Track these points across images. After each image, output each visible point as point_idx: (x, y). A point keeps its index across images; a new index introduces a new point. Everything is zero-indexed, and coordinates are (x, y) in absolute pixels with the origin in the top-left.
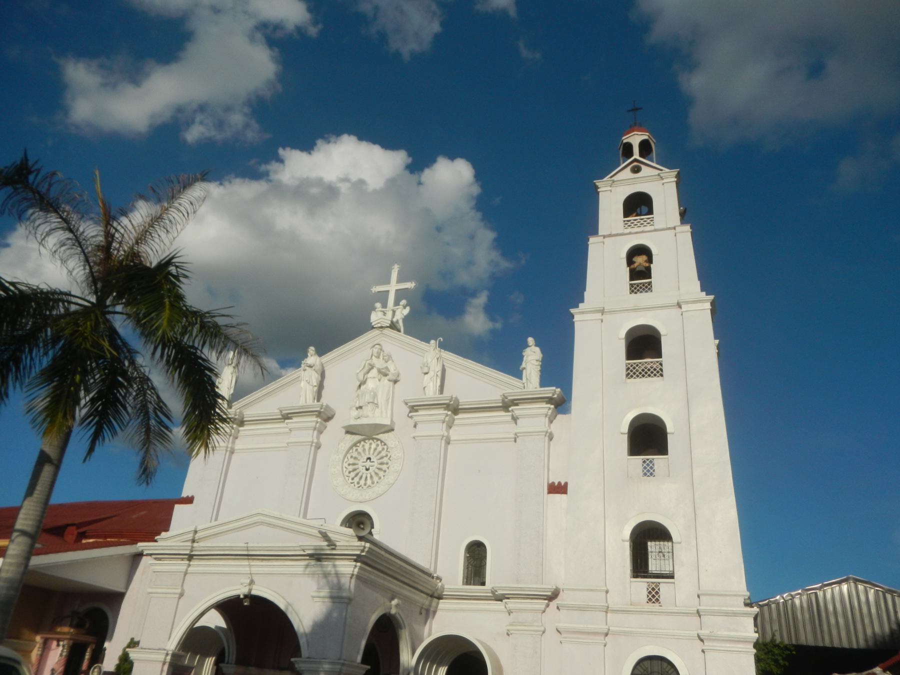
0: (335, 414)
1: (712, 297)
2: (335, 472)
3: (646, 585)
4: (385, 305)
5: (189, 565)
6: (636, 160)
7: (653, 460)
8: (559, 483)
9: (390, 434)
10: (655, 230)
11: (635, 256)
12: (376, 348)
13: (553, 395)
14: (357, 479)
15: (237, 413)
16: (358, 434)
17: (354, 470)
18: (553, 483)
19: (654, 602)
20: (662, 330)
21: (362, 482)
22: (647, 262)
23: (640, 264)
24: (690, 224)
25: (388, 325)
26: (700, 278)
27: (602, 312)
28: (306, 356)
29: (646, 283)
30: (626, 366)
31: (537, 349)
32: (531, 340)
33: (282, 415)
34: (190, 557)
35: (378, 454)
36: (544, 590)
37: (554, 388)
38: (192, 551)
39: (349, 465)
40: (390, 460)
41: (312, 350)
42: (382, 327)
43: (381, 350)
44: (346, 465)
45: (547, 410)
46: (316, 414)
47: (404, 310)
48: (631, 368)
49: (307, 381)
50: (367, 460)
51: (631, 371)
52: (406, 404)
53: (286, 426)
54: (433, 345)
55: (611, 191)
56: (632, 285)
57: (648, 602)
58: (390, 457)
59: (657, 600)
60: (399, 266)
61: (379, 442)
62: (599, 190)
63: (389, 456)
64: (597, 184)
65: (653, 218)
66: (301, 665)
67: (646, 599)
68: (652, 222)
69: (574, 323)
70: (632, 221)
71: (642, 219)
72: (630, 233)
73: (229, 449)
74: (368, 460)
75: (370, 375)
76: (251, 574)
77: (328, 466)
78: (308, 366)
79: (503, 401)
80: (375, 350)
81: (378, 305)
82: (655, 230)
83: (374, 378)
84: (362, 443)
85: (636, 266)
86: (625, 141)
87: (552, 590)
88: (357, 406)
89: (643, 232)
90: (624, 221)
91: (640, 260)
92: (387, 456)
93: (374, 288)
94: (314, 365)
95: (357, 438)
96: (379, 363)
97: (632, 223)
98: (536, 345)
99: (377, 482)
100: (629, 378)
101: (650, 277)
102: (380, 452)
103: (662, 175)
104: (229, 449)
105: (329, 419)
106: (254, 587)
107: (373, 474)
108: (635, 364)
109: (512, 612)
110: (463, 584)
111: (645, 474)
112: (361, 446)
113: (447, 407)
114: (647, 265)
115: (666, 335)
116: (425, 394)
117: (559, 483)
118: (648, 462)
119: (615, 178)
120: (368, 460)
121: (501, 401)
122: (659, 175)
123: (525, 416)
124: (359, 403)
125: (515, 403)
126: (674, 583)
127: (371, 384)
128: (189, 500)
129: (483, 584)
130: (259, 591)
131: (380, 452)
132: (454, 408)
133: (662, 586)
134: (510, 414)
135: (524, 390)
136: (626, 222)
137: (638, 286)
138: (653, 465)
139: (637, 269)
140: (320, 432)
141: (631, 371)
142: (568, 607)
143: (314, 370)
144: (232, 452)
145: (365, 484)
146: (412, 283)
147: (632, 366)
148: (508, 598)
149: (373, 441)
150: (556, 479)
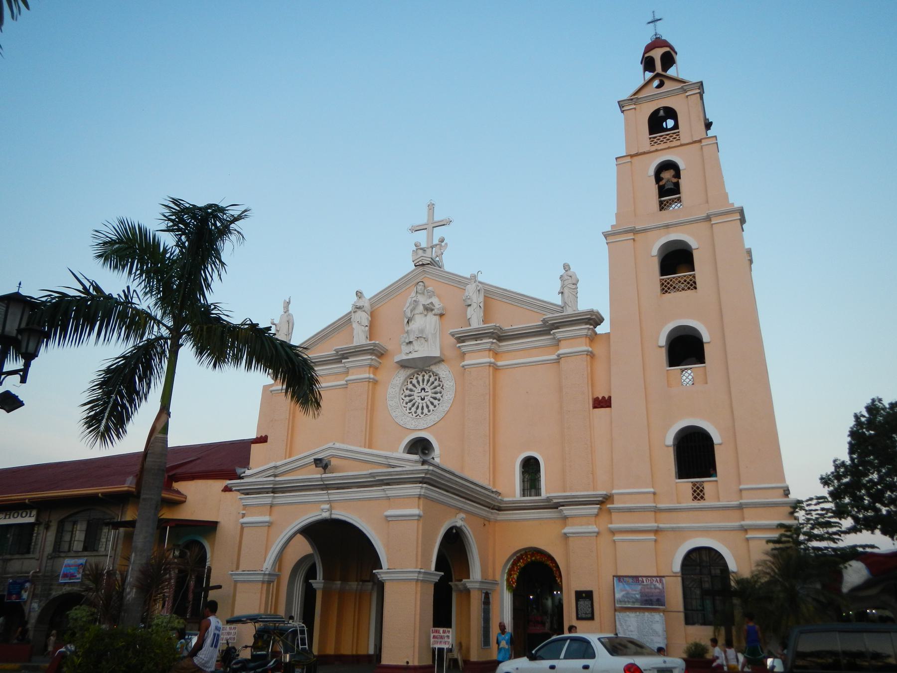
3: (690, 485)
6: (658, 75)
8: (604, 398)
10: (682, 145)
11: (662, 171)
12: (420, 285)
14: (414, 409)
17: (411, 401)
18: (598, 398)
19: (699, 500)
20: (693, 243)
21: (419, 411)
22: (675, 178)
23: (668, 180)
25: (429, 262)
29: (675, 199)
30: (661, 281)
34: (274, 491)
35: (431, 385)
39: (405, 396)
40: (443, 389)
42: (423, 265)
44: (403, 397)
48: (665, 284)
50: (421, 392)
51: (666, 286)
52: (453, 336)
53: (343, 365)
55: (635, 109)
56: (661, 203)
57: (693, 500)
58: (443, 386)
59: (702, 497)
63: (441, 386)
65: (679, 132)
66: (382, 576)
67: (692, 497)
68: (678, 137)
70: (658, 138)
72: (657, 150)
74: (423, 391)
75: (416, 311)
77: (386, 399)
82: (682, 145)
87: (603, 496)
88: (407, 341)
89: (669, 148)
90: (650, 138)
91: (667, 175)
92: (439, 385)
95: (409, 372)
96: (423, 300)
99: (433, 410)
100: (664, 293)
101: (679, 193)
102: (433, 383)
106: (333, 512)
107: (429, 403)
108: (668, 279)
110: (520, 496)
112: (414, 378)
113: (491, 335)
114: (675, 180)
116: (470, 325)
117: (604, 398)
119: (640, 95)
120: (423, 391)
122: (682, 88)
123: (566, 339)
125: (556, 326)
126: (716, 481)
129: (538, 493)
130: (340, 514)
131: (433, 383)
132: (501, 336)
133: (706, 485)
135: (563, 314)
136: (652, 139)
137: (667, 202)
139: (667, 187)
141: (666, 286)
142: (619, 509)
143: (364, 311)
145: (422, 413)
147: (666, 281)
148: (563, 506)
149: (426, 372)
150: (601, 394)
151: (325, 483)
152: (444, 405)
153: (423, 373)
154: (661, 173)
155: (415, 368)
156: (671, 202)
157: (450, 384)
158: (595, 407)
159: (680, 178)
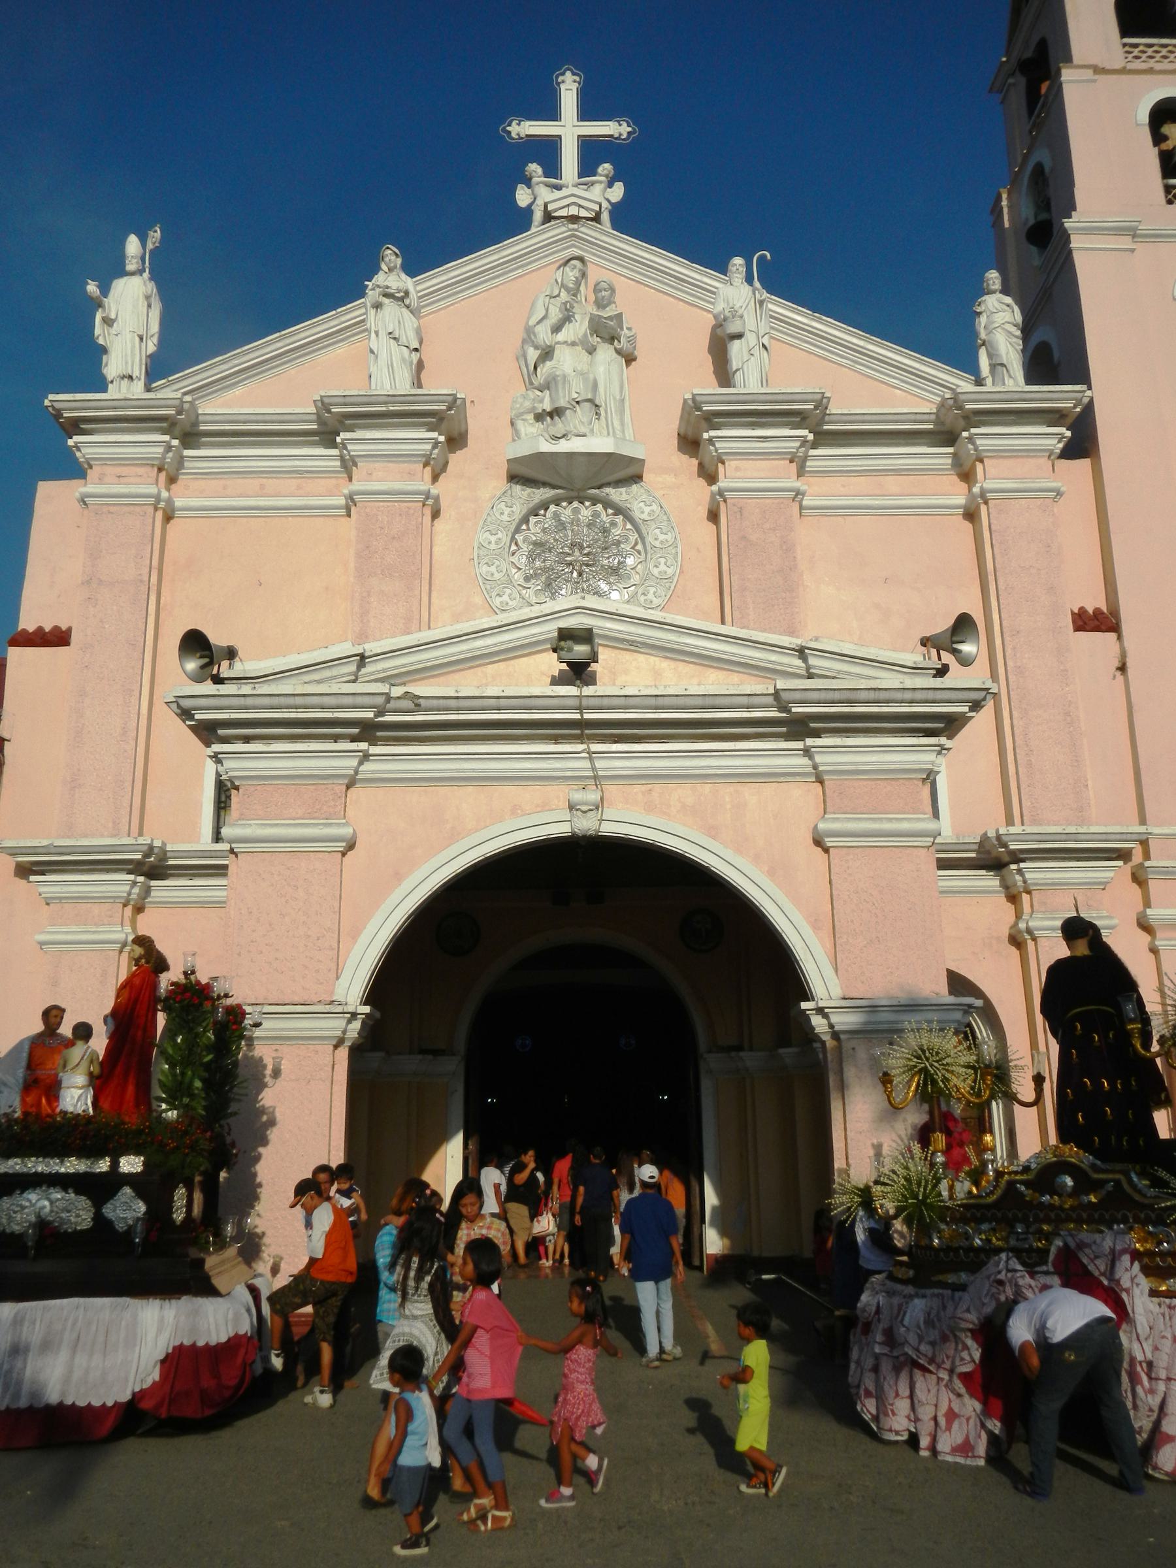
0: (467, 431)
2: (492, 574)
4: (552, 169)
5: (366, 757)
9: (634, 487)
12: (575, 267)
13: (1075, 407)
15: (186, 406)
16: (545, 484)
27: (1133, 233)
28: (376, 269)
31: (1008, 300)
32: (993, 277)
33: (320, 420)
34: (368, 731)
36: (1124, 837)
37: (1084, 387)
38: (380, 713)
41: (391, 256)
42: (574, 219)
43: (584, 275)
45: (1055, 441)
46: (432, 422)
47: (608, 190)
49: (390, 333)
53: (335, 452)
54: (741, 269)
56: (1168, 189)
60: (577, 78)
61: (599, 507)
69: (1070, 252)
70: (1141, 48)
72: (1151, 71)
73: (162, 505)
75: (560, 337)
76: (595, 777)
78: (386, 295)
79: (937, 414)
80: (571, 274)
81: (534, 168)
83: (573, 344)
84: (552, 508)
85: (1171, 147)
90: (1125, 45)
93: (514, 123)
94: (407, 293)
97: (1143, 52)
98: (1005, 291)
104: (162, 505)
105: (456, 441)
106: (608, 813)
109: (1029, 892)
112: (549, 514)
121: (933, 417)
123: (999, 454)
124: (552, 399)
127: (566, 361)
128: (58, 638)
134: (951, 450)
140: (435, 478)
143: (408, 307)
144: (168, 518)
146: (620, 125)
148: (1023, 861)
151: (586, 716)
152: (652, 590)
153: (576, 504)
155: (554, 487)
157: (662, 537)
158: (1078, 628)
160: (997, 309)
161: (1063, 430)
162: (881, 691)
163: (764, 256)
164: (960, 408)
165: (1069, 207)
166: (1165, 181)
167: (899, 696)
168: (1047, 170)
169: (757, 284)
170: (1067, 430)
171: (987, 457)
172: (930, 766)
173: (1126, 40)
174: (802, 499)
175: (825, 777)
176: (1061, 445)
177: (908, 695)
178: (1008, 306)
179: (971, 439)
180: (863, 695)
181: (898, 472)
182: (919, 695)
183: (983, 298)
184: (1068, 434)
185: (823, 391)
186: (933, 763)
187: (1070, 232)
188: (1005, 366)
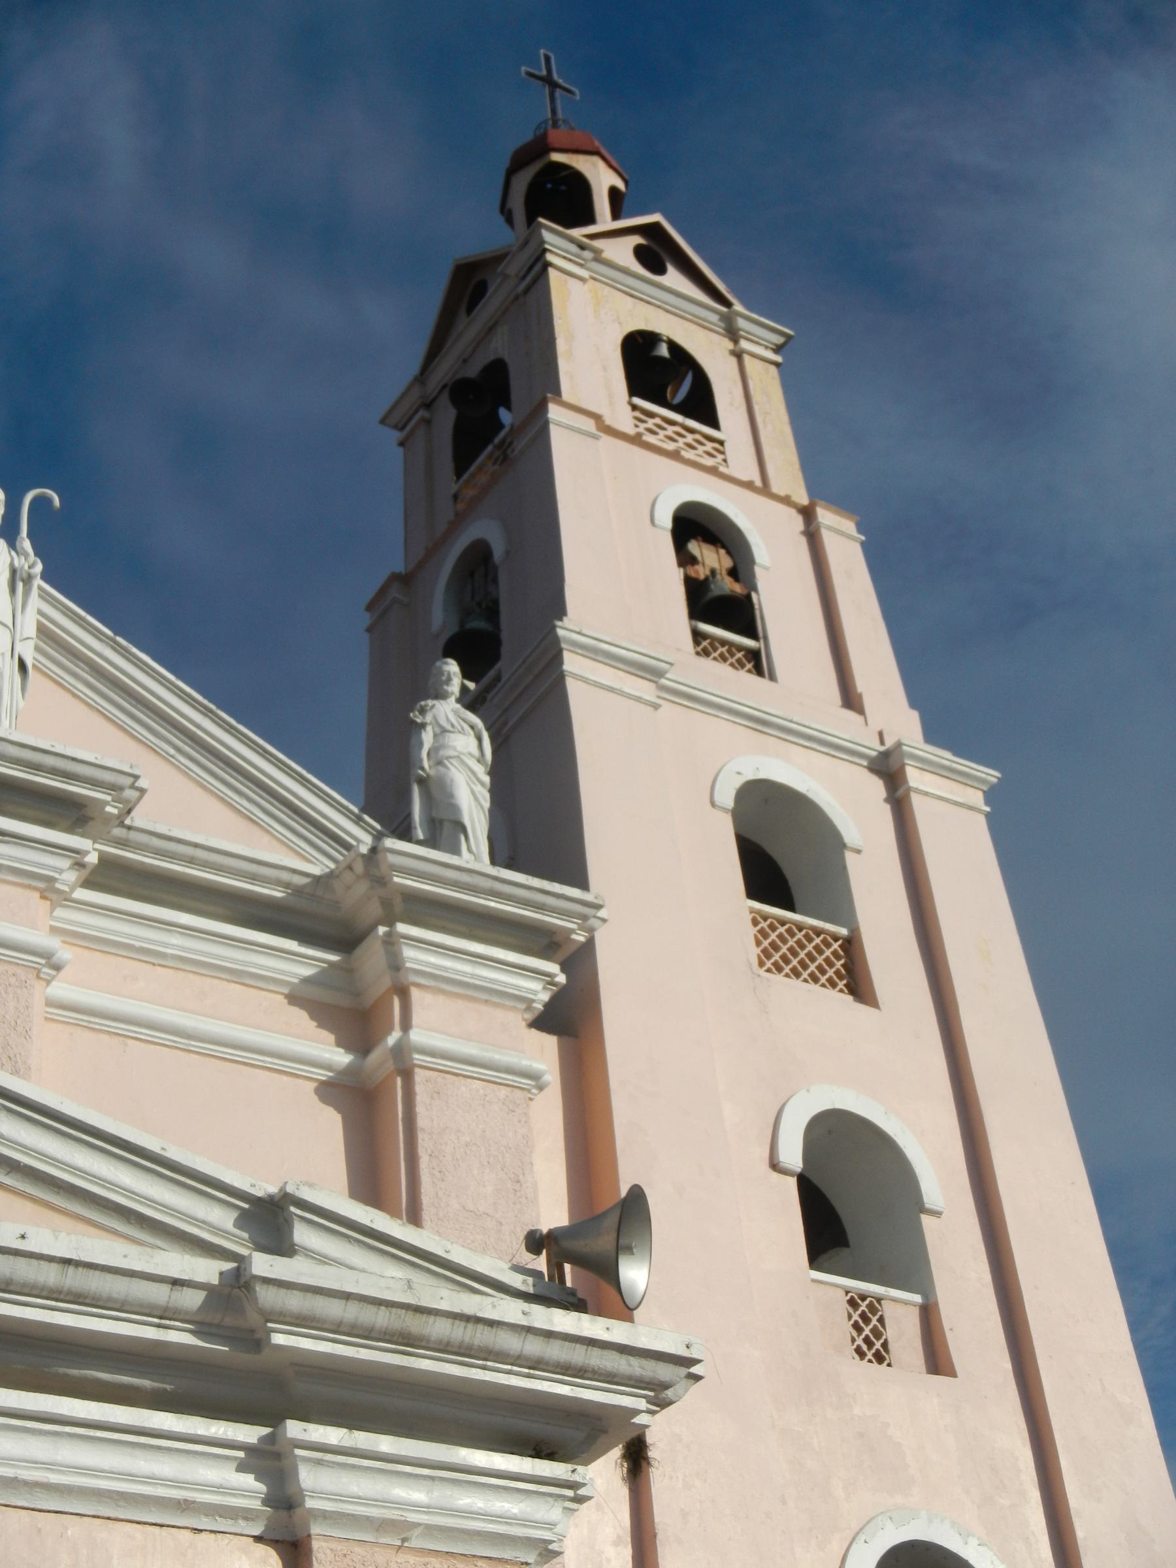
1: (992, 775)
7: (879, 1300)
10: (749, 485)
24: (858, 518)
26: (914, 703)
29: (740, 648)
56: (697, 636)
62: (550, 257)
64: (547, 236)
65: (721, 443)
68: (720, 457)
69: (561, 678)
71: (691, 431)
72: (675, 455)
85: (702, 577)
86: (557, 157)
89: (713, 471)
90: (634, 407)
91: (710, 558)
103: (741, 323)
111: (860, 1353)
114: (738, 588)
115: (858, 852)
118: (863, 1306)
138: (881, 1320)
139: (715, 591)
154: (687, 540)
156: (724, 649)
159: (755, 589)
160: (453, 726)
161: (553, 968)
162: (480, 1327)
163: (47, 501)
164: (381, 881)
165: (560, 610)
166: (694, 622)
167: (511, 1343)
168: (498, 552)
169: (27, 545)
170: (563, 970)
171: (418, 985)
172: (547, 1535)
173: (637, 401)
174: (53, 978)
175: (316, 1529)
176: (545, 997)
177: (534, 1347)
178: (472, 727)
179: (391, 941)
180: (440, 1329)
181: (238, 976)
182: (556, 1352)
183: (430, 702)
184: (562, 979)
185: (136, 772)
186: (550, 1526)
187: (563, 646)
188: (464, 830)
